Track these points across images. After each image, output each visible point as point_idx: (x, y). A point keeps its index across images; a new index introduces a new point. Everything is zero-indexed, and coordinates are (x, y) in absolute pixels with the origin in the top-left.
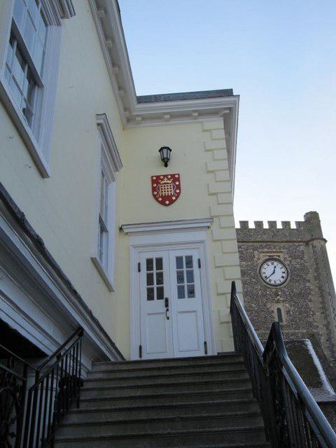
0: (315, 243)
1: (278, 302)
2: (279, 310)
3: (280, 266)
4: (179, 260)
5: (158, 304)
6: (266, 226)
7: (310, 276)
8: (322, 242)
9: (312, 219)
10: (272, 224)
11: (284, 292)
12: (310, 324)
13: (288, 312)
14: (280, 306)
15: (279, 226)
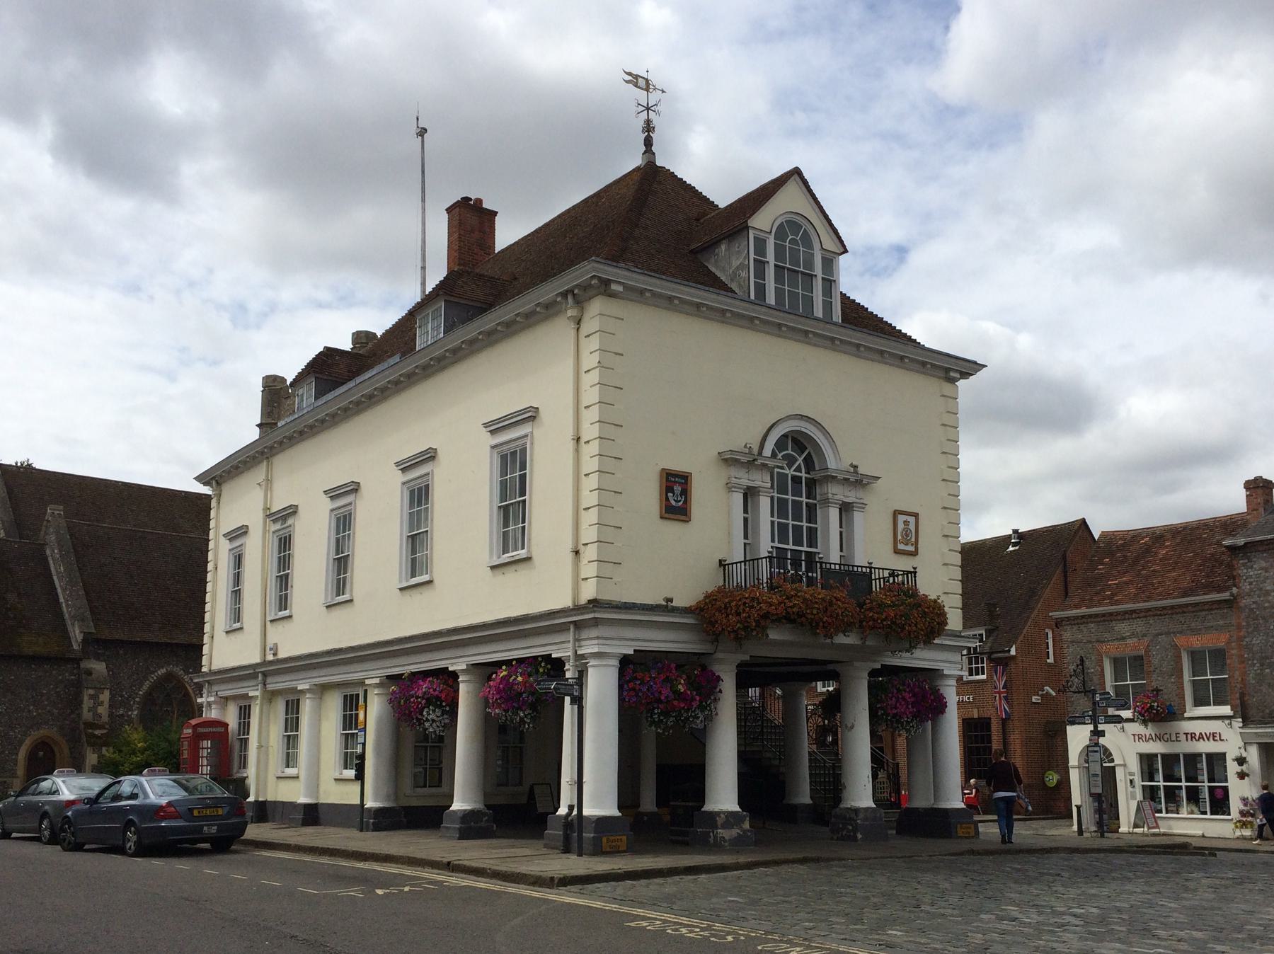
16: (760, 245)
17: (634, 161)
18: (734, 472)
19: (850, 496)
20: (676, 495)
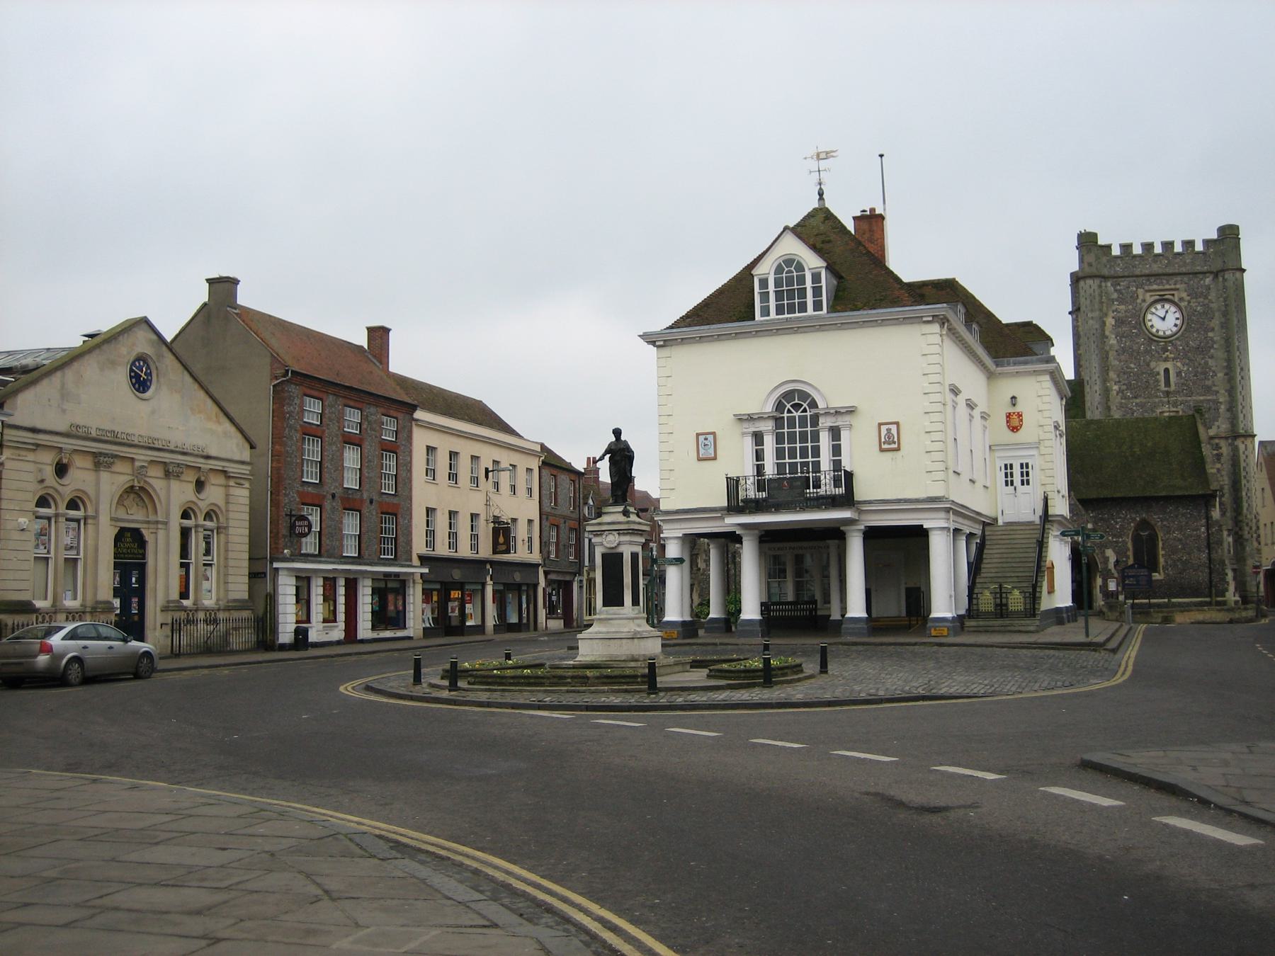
1: (1166, 360)
2: (1167, 371)
3: (1173, 309)
4: (1022, 465)
5: (1010, 488)
6: (1158, 249)
7: (1215, 323)
8: (1238, 274)
9: (1229, 235)
10: (1168, 245)
11: (1175, 346)
12: (1208, 390)
13: (1179, 374)
14: (1169, 365)
15: (1178, 248)
16: (764, 283)
17: (815, 204)
18: (746, 425)
19: (839, 422)
20: (707, 446)
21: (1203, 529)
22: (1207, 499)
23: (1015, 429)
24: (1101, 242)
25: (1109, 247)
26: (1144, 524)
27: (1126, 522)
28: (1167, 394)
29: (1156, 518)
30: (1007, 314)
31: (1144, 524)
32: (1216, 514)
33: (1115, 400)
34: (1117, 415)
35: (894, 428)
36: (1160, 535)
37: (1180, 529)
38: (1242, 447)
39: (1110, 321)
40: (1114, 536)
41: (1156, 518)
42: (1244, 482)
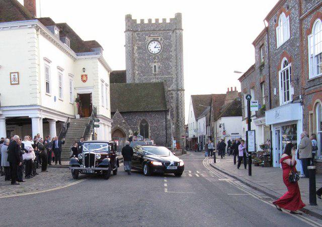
0: (177, 31)
1: (155, 62)
2: (155, 66)
8: (181, 31)
9: (178, 17)
11: (158, 57)
12: (169, 73)
13: (159, 67)
14: (156, 64)
21: (164, 123)
22: (166, 112)
23: (84, 81)
24: (133, 18)
25: (136, 20)
26: (144, 121)
27: (138, 120)
28: (155, 75)
29: (148, 119)
30: (85, 37)
31: (144, 121)
32: (169, 117)
33: (137, 77)
34: (137, 81)
35: (16, 74)
36: (149, 125)
37: (157, 123)
38: (180, 94)
39: (136, 48)
40: (134, 125)
41: (148, 119)
42: (180, 106)
